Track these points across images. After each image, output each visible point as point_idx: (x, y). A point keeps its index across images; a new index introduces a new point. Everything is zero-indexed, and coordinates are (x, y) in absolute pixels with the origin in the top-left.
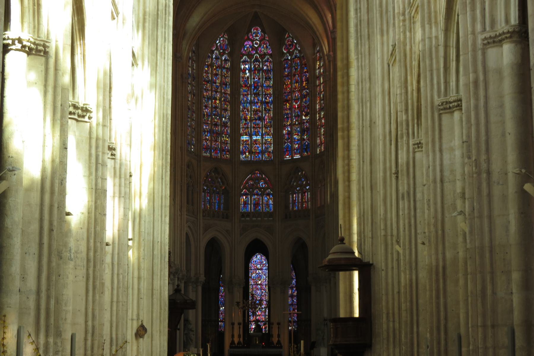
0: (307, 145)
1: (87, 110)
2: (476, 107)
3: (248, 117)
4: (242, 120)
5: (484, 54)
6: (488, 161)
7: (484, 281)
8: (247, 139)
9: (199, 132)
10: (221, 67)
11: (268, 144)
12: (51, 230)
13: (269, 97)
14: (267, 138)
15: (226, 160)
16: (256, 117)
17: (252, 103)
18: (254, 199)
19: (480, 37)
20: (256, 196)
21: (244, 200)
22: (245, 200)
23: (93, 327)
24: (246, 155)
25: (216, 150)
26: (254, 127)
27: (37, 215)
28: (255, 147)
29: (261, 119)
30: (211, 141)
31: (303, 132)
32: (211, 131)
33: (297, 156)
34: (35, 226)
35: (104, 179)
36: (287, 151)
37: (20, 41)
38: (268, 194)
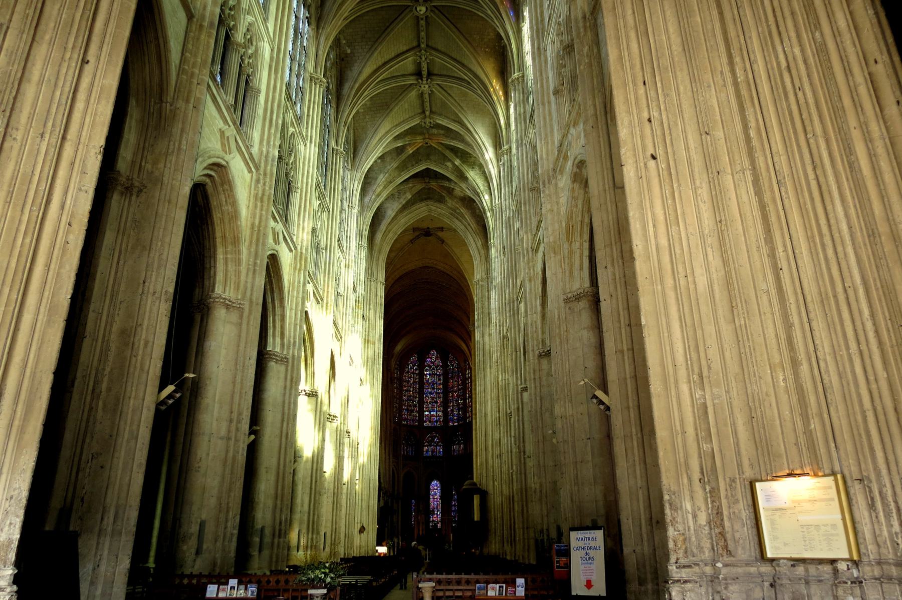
1: (336, 417)
2: (518, 420)
5: (522, 395)
6: (524, 446)
7: (523, 506)
9: (400, 410)
10: (413, 373)
12: (316, 481)
15: (416, 426)
17: (430, 393)
19: (520, 387)
23: (336, 529)
25: (410, 420)
27: (310, 474)
29: (436, 402)
30: (407, 415)
31: (459, 410)
32: (407, 410)
33: (456, 424)
34: (309, 480)
35: (343, 451)
37: (305, 391)
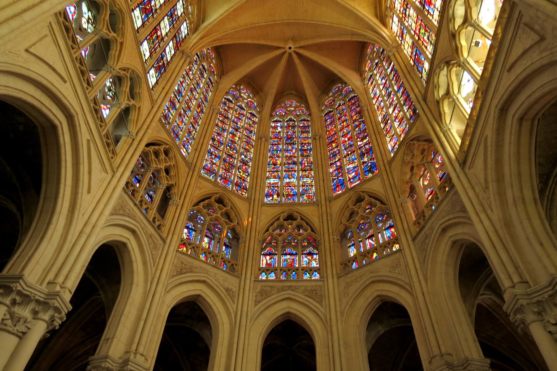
0: (371, 166)
3: (279, 163)
4: (269, 165)
8: (276, 181)
11: (307, 186)
13: (307, 146)
14: (305, 181)
16: (290, 162)
18: (286, 260)
20: (288, 257)
21: (267, 262)
22: (269, 262)
24: (273, 198)
26: (285, 171)
28: (288, 189)
36: (337, 186)
38: (310, 254)
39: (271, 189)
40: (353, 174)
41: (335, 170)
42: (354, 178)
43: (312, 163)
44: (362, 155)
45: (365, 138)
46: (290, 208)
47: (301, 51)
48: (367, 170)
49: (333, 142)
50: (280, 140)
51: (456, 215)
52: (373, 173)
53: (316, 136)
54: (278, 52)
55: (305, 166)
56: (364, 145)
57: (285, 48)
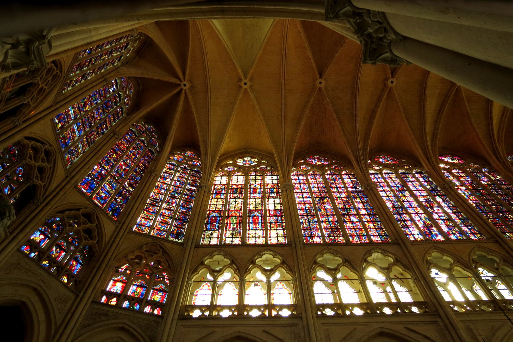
11: (76, 151)
16: (90, 119)
28: (69, 134)
36: (87, 184)
39: (64, 115)
40: (104, 195)
41: (98, 172)
42: (101, 197)
43: (94, 142)
44: (120, 194)
45: (132, 187)
46: (57, 150)
47: (183, 96)
48: (112, 207)
49: (117, 154)
50: (104, 97)
51: (143, 334)
52: (113, 215)
53: (118, 135)
54: (180, 74)
55: (90, 137)
56: (127, 190)
57: (184, 80)
